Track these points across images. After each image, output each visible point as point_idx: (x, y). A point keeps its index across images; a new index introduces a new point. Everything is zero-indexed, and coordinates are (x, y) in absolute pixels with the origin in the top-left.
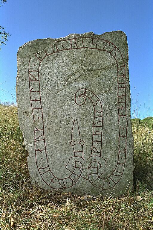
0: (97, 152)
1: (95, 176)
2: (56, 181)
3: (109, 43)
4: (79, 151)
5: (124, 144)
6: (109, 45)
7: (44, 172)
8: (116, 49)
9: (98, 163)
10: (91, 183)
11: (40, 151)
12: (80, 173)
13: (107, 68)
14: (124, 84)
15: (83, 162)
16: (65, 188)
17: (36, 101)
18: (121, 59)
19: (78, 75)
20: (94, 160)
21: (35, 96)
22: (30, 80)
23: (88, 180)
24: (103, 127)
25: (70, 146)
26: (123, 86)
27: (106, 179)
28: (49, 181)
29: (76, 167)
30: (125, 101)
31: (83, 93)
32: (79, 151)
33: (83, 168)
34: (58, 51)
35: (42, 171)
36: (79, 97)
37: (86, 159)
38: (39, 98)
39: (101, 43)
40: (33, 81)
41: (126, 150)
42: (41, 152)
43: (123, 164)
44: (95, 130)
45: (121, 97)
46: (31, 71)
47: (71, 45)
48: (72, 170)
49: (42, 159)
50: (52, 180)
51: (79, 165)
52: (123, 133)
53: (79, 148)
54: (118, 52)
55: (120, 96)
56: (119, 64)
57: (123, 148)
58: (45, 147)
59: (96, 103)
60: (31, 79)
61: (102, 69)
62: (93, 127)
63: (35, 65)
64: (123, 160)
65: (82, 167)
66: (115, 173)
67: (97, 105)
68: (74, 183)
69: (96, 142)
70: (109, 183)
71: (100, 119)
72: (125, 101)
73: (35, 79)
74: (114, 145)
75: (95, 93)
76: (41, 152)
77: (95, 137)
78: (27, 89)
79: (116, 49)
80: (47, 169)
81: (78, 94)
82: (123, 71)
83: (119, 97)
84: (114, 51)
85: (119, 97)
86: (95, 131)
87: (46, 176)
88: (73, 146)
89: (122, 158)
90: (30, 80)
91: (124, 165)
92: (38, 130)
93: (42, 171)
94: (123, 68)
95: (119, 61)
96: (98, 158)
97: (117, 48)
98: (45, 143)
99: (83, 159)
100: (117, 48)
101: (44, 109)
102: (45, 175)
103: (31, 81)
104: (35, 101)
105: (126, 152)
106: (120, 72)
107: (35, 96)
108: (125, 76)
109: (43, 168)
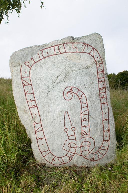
0: (86, 134)
3: (88, 46)
4: (72, 135)
5: (107, 125)
6: (88, 47)
7: (46, 154)
8: (94, 49)
9: (88, 142)
10: (84, 158)
11: (41, 139)
14: (103, 79)
16: (64, 163)
17: (31, 101)
19: (64, 75)
20: (84, 141)
21: (30, 97)
22: (24, 85)
23: (81, 156)
24: (89, 114)
25: (64, 132)
26: (103, 79)
29: (70, 147)
30: (106, 92)
31: (70, 90)
32: (72, 135)
33: (76, 147)
34: (44, 58)
35: (44, 154)
37: (78, 141)
39: (80, 47)
40: (26, 85)
41: (109, 130)
43: (108, 141)
44: (83, 117)
45: (102, 89)
46: (23, 77)
47: (55, 51)
48: (68, 150)
49: (43, 145)
50: (53, 159)
51: (73, 145)
52: (106, 117)
53: (72, 133)
54: (95, 52)
55: (100, 89)
56: (97, 62)
57: (107, 128)
58: (44, 136)
59: (81, 97)
61: (84, 68)
62: (81, 115)
64: (108, 137)
65: (76, 147)
67: (82, 98)
69: (85, 127)
70: (98, 156)
72: (106, 92)
73: (28, 83)
74: (100, 127)
75: (80, 89)
77: (84, 123)
79: (94, 49)
80: (49, 152)
81: (66, 92)
82: (101, 68)
83: (100, 89)
84: (92, 51)
85: (100, 89)
87: (48, 157)
88: (66, 132)
89: (106, 136)
91: (108, 141)
92: (37, 123)
95: (97, 60)
96: (87, 139)
97: (94, 49)
98: (44, 133)
99: (76, 141)
100: (94, 49)
102: (47, 156)
103: (25, 85)
104: (30, 102)
105: (109, 132)
106: (99, 69)
107: (30, 97)
108: (104, 71)
109: (45, 152)
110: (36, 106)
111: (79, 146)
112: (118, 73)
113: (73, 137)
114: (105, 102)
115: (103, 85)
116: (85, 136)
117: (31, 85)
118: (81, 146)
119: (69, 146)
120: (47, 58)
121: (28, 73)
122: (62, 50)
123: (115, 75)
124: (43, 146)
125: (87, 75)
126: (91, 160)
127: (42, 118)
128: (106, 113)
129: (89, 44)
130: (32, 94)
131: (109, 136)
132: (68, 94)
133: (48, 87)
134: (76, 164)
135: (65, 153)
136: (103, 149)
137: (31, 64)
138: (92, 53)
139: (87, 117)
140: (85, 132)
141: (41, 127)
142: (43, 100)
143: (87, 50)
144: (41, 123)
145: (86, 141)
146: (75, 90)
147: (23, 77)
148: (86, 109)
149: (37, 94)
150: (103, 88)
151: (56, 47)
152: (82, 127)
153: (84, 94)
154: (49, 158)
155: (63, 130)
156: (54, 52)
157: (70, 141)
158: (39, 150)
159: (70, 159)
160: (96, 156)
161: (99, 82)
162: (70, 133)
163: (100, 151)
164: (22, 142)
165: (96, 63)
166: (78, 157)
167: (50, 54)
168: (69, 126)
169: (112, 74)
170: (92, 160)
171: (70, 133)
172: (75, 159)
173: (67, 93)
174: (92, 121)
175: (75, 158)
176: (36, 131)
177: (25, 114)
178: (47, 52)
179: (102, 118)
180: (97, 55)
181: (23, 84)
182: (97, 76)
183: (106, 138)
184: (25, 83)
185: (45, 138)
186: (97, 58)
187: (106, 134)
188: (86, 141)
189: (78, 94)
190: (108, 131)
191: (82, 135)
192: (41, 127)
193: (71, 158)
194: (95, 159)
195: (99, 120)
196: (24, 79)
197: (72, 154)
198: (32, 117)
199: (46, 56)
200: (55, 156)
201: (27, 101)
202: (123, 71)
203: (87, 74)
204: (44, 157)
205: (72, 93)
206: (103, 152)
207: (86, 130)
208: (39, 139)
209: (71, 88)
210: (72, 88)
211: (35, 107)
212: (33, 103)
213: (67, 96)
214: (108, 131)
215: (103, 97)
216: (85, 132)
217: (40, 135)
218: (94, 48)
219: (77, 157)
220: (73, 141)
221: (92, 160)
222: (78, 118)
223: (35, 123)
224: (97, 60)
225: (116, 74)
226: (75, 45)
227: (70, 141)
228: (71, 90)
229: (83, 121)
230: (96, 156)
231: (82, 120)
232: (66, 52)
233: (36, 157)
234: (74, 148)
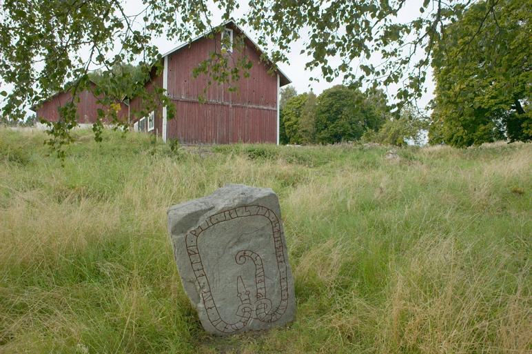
1: (263, 315)
2: (230, 328)
5: (285, 283)
13: (263, 229)
19: (236, 240)
28: (223, 329)
35: (215, 323)
39: (254, 210)
44: (258, 279)
77: (259, 285)
90: (190, 254)
102: (218, 325)
107: (197, 266)
111: (255, 309)
113: (248, 301)
114: (283, 260)
121: (194, 242)
127: (211, 286)
133: (218, 254)
137: (198, 232)
138: (267, 215)
139: (262, 278)
142: (212, 267)
149: (205, 263)
154: (220, 326)
160: (273, 317)
164: (189, 314)
167: (219, 220)
173: (241, 256)
174: (268, 281)
175: (251, 322)
182: (272, 237)
183: (284, 298)
184: (191, 253)
201: (194, 271)
203: (262, 236)
207: (262, 291)
217: (209, 304)
220: (247, 305)
222: (252, 282)
226: (248, 208)
228: (244, 253)
230: (273, 317)
233: (205, 328)
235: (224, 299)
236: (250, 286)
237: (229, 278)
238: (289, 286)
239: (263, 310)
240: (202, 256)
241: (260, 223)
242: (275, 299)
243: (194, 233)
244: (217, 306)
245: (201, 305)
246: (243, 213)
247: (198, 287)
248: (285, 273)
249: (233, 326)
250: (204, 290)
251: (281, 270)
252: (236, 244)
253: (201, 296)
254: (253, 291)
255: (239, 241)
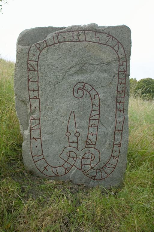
0: (91, 144)
1: (88, 167)
3: (113, 38)
4: (74, 142)
5: (119, 137)
6: (112, 40)
7: (38, 160)
8: (119, 44)
9: (92, 154)
10: (84, 173)
11: (35, 139)
12: (74, 163)
13: (109, 63)
15: (77, 152)
16: (58, 176)
17: (33, 90)
18: (124, 54)
19: (78, 67)
20: (88, 151)
21: (33, 86)
22: (29, 70)
23: (81, 170)
24: (99, 120)
25: (65, 136)
26: (123, 81)
27: (99, 170)
29: (69, 157)
31: (82, 87)
32: (74, 142)
33: (77, 158)
34: (59, 42)
35: (36, 158)
36: (78, 90)
38: (37, 88)
40: (31, 71)
41: (121, 144)
42: (36, 140)
43: (116, 157)
44: (92, 122)
45: (120, 92)
47: (73, 37)
48: (66, 159)
49: (37, 147)
50: (45, 168)
51: (73, 155)
52: (119, 127)
53: (75, 139)
54: (121, 46)
56: (120, 60)
57: (118, 142)
58: (41, 136)
59: (94, 97)
60: (29, 69)
61: (104, 63)
62: (90, 119)
63: (34, 55)
66: (108, 165)
67: (95, 98)
68: (67, 172)
69: (92, 135)
71: (97, 112)
75: (94, 88)
76: (36, 140)
77: (91, 130)
78: (25, 79)
79: (119, 44)
80: (42, 157)
82: (124, 67)
84: (117, 46)
85: (118, 92)
86: (91, 124)
88: (68, 136)
89: (116, 151)
90: (29, 70)
91: (117, 158)
92: (34, 119)
93: (36, 158)
94: (125, 63)
95: (121, 56)
96: (92, 150)
97: (120, 44)
98: (40, 132)
99: (78, 150)
100: (120, 44)
101: (42, 100)
103: (30, 71)
104: (33, 91)
105: (120, 146)
106: (121, 67)
107: (33, 86)
108: (126, 72)
109: (37, 156)
110: (38, 97)
111: (81, 157)
112: (140, 80)
113: (74, 145)
114: (122, 108)
115: (123, 88)
116: (90, 145)
117: (38, 71)
118: (83, 158)
119: (68, 155)
120: (62, 43)
121: (37, 56)
122: (82, 38)
123: (136, 81)
124: (36, 148)
125: (106, 72)
126: (91, 178)
128: (120, 123)
129: (114, 36)
130: (37, 83)
131: (120, 152)
132: (79, 91)
133: (57, 78)
134: (72, 179)
135: (62, 162)
136: (109, 166)
138: (116, 48)
139: (96, 122)
140: (91, 141)
141: (39, 125)
142: (48, 91)
143: (111, 42)
144: (39, 119)
145: (89, 153)
146: (88, 87)
147: (30, 61)
148: (97, 112)
149: (42, 84)
150: (122, 91)
151: (76, 33)
152: (88, 134)
153: (98, 94)
154: (41, 164)
155: (64, 133)
156: (72, 38)
157: (71, 149)
158: (30, 153)
159: (67, 172)
160: (98, 174)
161: (118, 83)
162: (73, 139)
163: (104, 169)
165: (119, 61)
166: (76, 171)
167: (67, 39)
168: (72, 129)
169: (133, 79)
170: (93, 178)
171: (73, 139)
172: (72, 173)
173: (79, 89)
175: (73, 171)
176: (32, 129)
177: (23, 105)
178: (63, 36)
179: (114, 128)
180: (121, 50)
181: (28, 68)
182: (117, 76)
183: (116, 154)
185: (41, 139)
186: (121, 54)
187: (116, 148)
188: (89, 153)
189: (91, 92)
190: (118, 146)
191: (86, 144)
192: (39, 125)
193: (67, 170)
194: (97, 178)
195: (110, 130)
196: (32, 62)
197: (69, 166)
198: (31, 111)
199: (62, 41)
200: (48, 165)
202: (147, 78)
203: (106, 71)
204: (35, 162)
205: (85, 91)
206: (109, 171)
207: (93, 138)
208: (34, 138)
209: (83, 84)
210: (85, 84)
211: (37, 98)
212: (36, 94)
213: (77, 93)
214: (118, 146)
215: (120, 103)
216: (91, 141)
217: (36, 134)
218: (119, 42)
219: (75, 170)
220: (74, 150)
221: (93, 178)
222: (84, 123)
223: (32, 118)
224: (120, 57)
225: (138, 79)
226: (98, 35)
227: (71, 149)
228: (84, 86)
229: (91, 127)
230: (98, 174)
231: (90, 126)
232: (85, 41)
233: (25, 161)
234: (73, 158)
235: (51, 133)
236: (81, 127)
237: (62, 111)
238: (123, 142)
239: (88, 162)
240: (40, 75)
241: (107, 55)
242: (106, 154)
243: (38, 46)
244: (43, 139)
245: (27, 133)
246: (91, 38)
247: (29, 111)
248: (121, 124)
249: (54, 169)
250: (34, 116)
251: (119, 119)
252: (78, 72)
253: (29, 122)
254: (83, 134)
255: (80, 71)
